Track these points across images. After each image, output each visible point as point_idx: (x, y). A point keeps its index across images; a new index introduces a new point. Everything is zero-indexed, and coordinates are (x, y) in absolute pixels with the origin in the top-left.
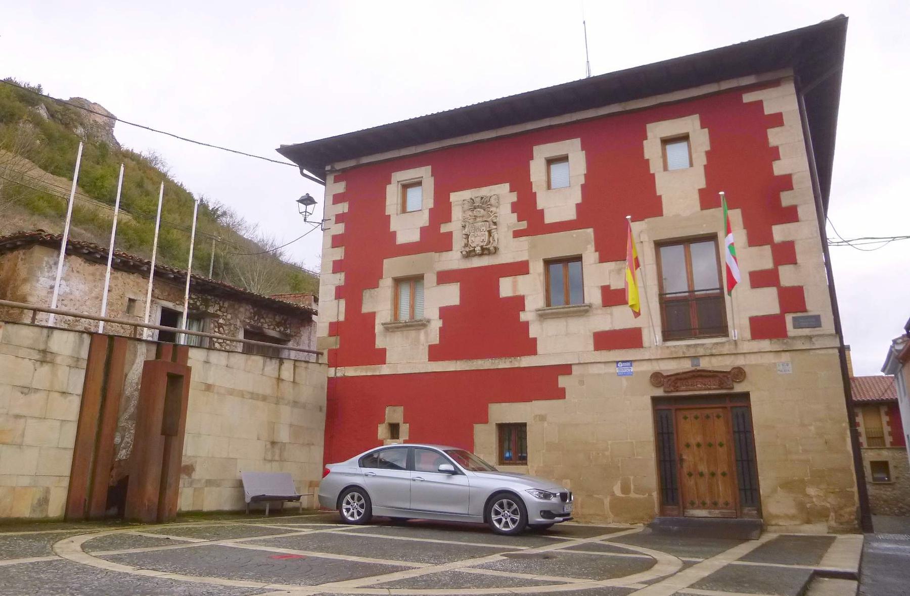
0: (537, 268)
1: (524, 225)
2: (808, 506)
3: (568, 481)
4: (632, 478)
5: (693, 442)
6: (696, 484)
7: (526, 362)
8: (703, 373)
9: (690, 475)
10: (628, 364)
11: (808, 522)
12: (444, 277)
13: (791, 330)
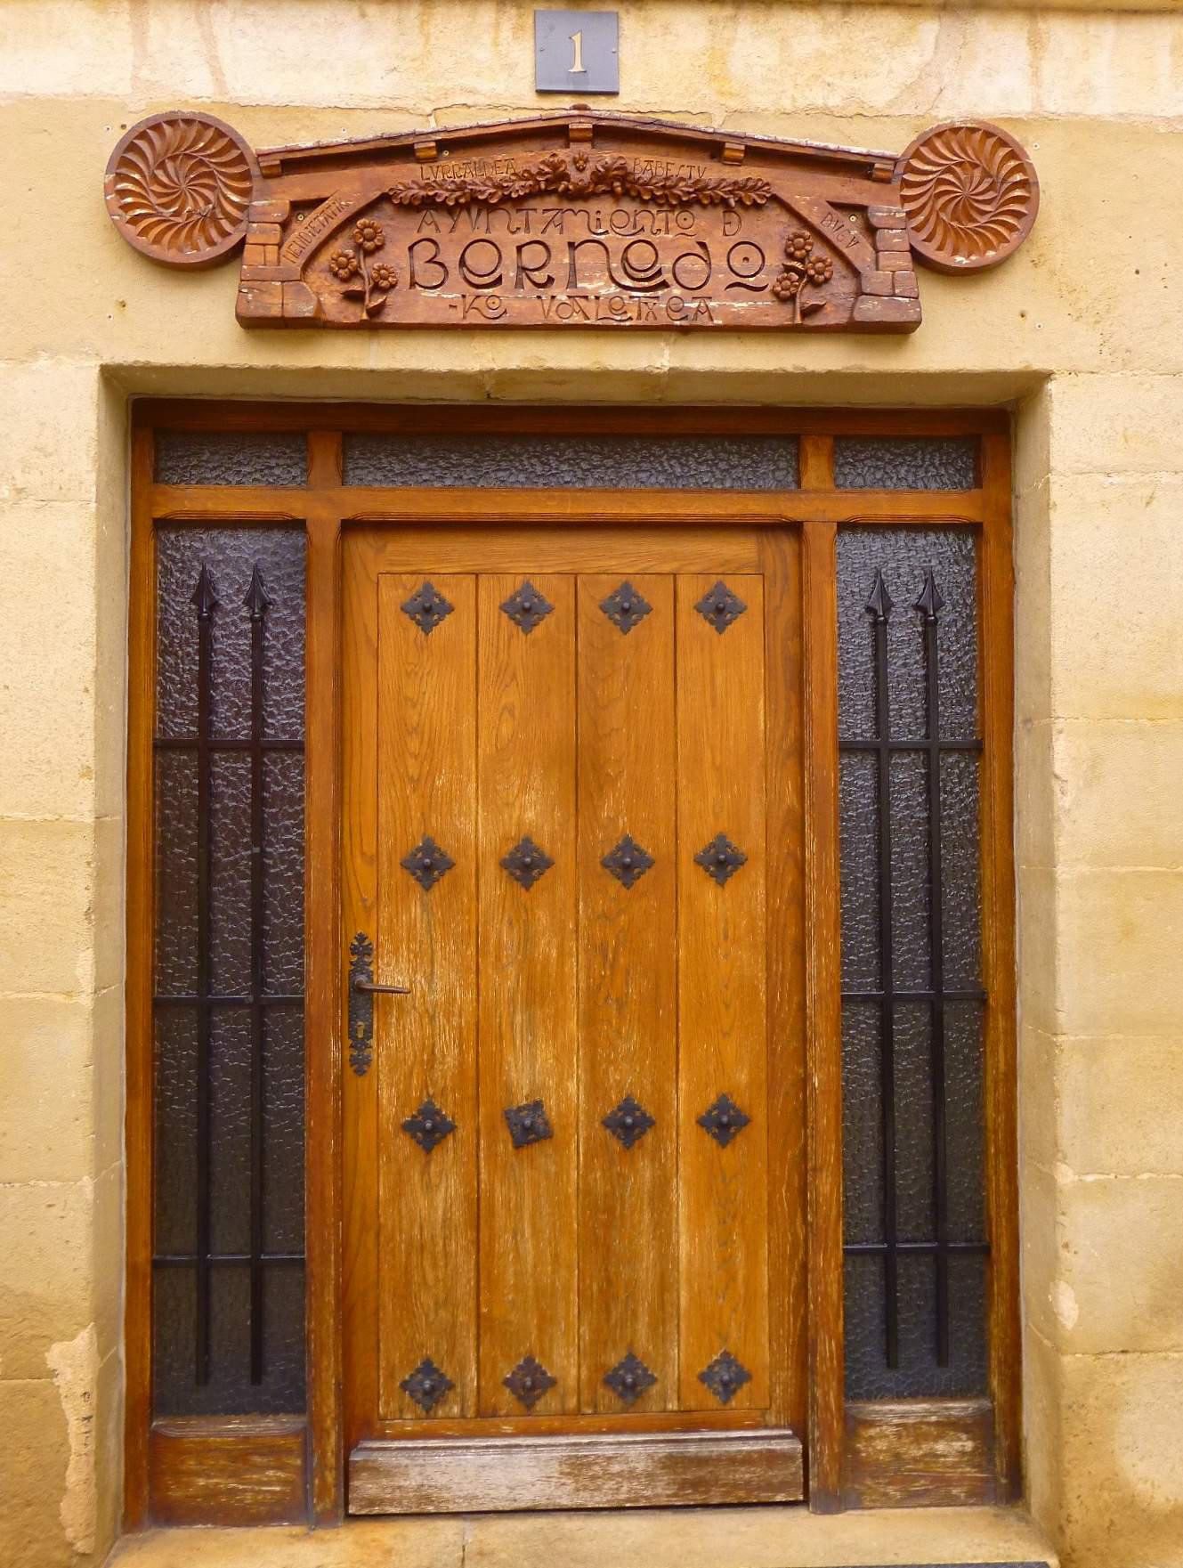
5: (476, 830)
6: (478, 1212)
8: (645, 164)
9: (429, 1130)
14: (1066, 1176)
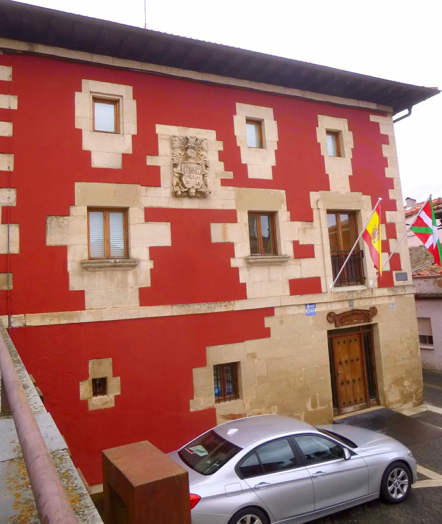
0: (243, 218)
1: (230, 175)
2: (405, 392)
3: (276, 407)
4: (318, 395)
5: (343, 360)
7: (239, 305)
9: (342, 384)
10: (313, 306)
11: (405, 403)
12: (153, 215)
13: (396, 283)
14: (384, 380)
